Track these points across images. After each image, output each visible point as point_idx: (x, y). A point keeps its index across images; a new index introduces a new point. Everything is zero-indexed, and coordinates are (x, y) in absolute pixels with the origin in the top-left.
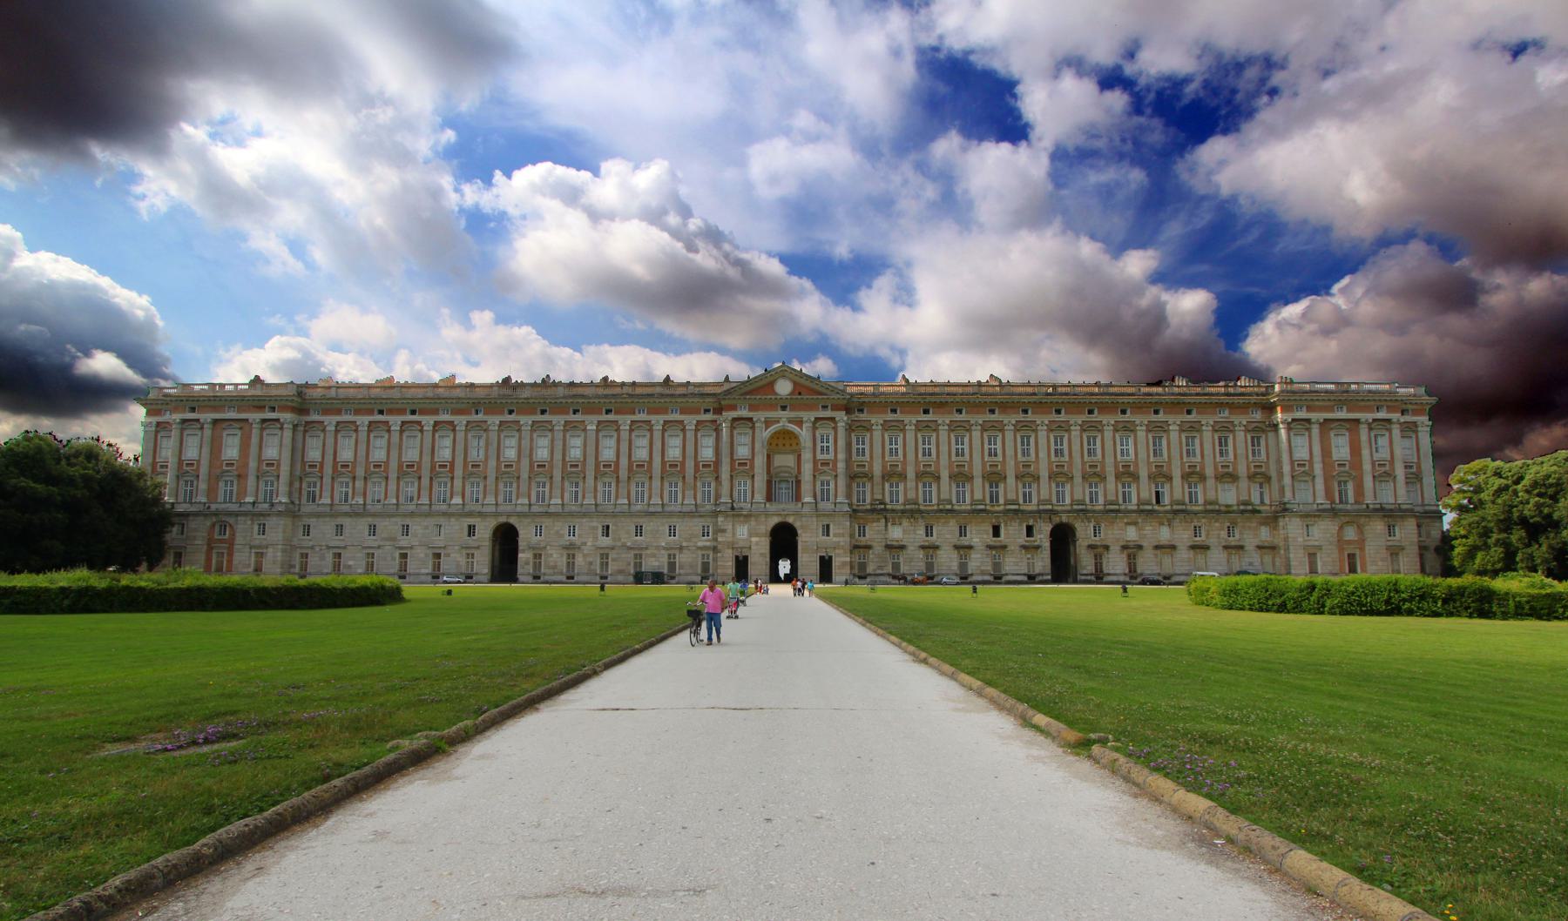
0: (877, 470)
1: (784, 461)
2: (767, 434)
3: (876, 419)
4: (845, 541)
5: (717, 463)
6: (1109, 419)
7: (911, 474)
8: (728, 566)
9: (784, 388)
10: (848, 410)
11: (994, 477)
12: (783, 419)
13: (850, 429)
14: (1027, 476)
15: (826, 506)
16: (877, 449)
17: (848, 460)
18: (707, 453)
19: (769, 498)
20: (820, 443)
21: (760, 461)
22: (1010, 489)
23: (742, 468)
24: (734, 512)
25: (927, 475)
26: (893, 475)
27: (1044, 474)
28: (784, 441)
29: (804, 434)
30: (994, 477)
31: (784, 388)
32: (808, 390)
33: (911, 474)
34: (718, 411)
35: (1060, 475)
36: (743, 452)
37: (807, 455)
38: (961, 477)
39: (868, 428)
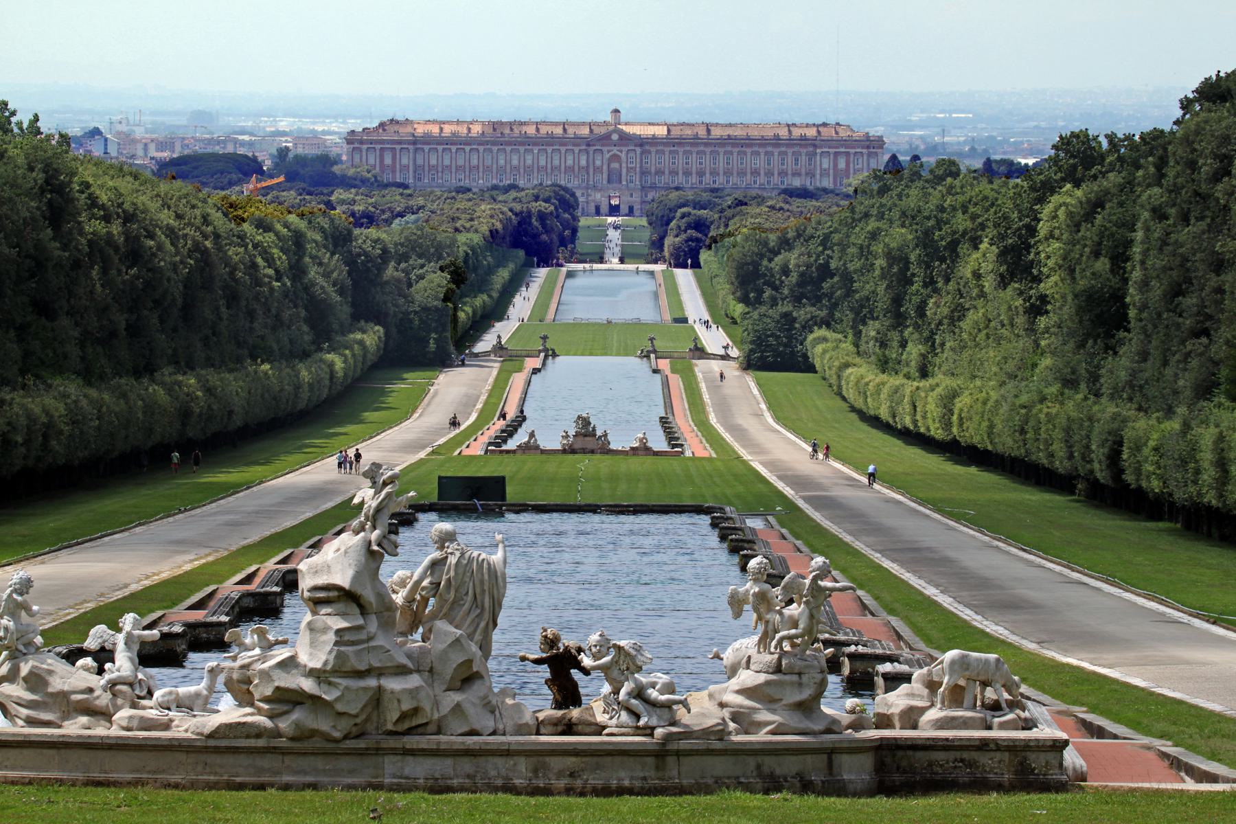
0: (653, 171)
1: (615, 165)
2: (608, 156)
3: (653, 149)
4: (638, 200)
5: (588, 167)
6: (749, 150)
7: (667, 172)
8: (593, 210)
9: (615, 137)
10: (641, 145)
11: (701, 174)
12: (615, 150)
13: (642, 153)
14: (714, 173)
15: (632, 185)
16: (653, 162)
17: (641, 167)
18: (583, 163)
19: (609, 182)
20: (629, 159)
21: (605, 167)
22: (707, 179)
23: (598, 170)
24: (595, 188)
25: (674, 173)
26: (659, 172)
27: (721, 173)
28: (615, 158)
29: (623, 156)
30: (701, 174)
31: (615, 137)
32: (625, 138)
33: (667, 172)
34: (588, 145)
35: (728, 173)
36: (598, 163)
37: (624, 165)
38: (687, 173)
39: (649, 152)
